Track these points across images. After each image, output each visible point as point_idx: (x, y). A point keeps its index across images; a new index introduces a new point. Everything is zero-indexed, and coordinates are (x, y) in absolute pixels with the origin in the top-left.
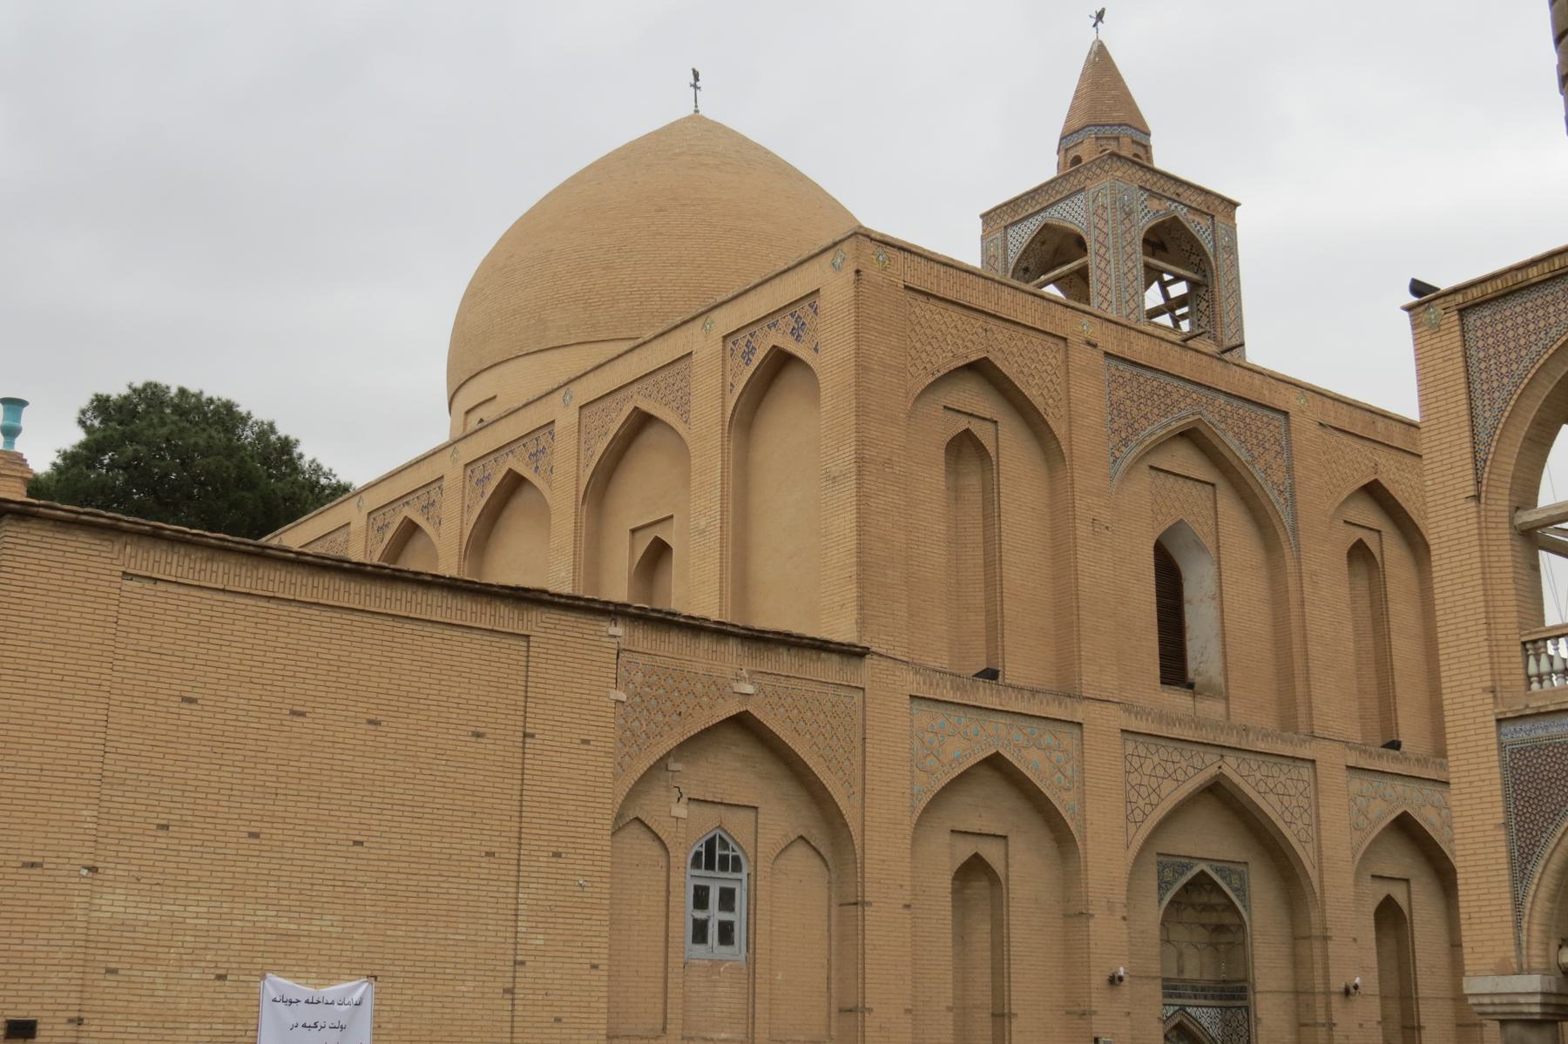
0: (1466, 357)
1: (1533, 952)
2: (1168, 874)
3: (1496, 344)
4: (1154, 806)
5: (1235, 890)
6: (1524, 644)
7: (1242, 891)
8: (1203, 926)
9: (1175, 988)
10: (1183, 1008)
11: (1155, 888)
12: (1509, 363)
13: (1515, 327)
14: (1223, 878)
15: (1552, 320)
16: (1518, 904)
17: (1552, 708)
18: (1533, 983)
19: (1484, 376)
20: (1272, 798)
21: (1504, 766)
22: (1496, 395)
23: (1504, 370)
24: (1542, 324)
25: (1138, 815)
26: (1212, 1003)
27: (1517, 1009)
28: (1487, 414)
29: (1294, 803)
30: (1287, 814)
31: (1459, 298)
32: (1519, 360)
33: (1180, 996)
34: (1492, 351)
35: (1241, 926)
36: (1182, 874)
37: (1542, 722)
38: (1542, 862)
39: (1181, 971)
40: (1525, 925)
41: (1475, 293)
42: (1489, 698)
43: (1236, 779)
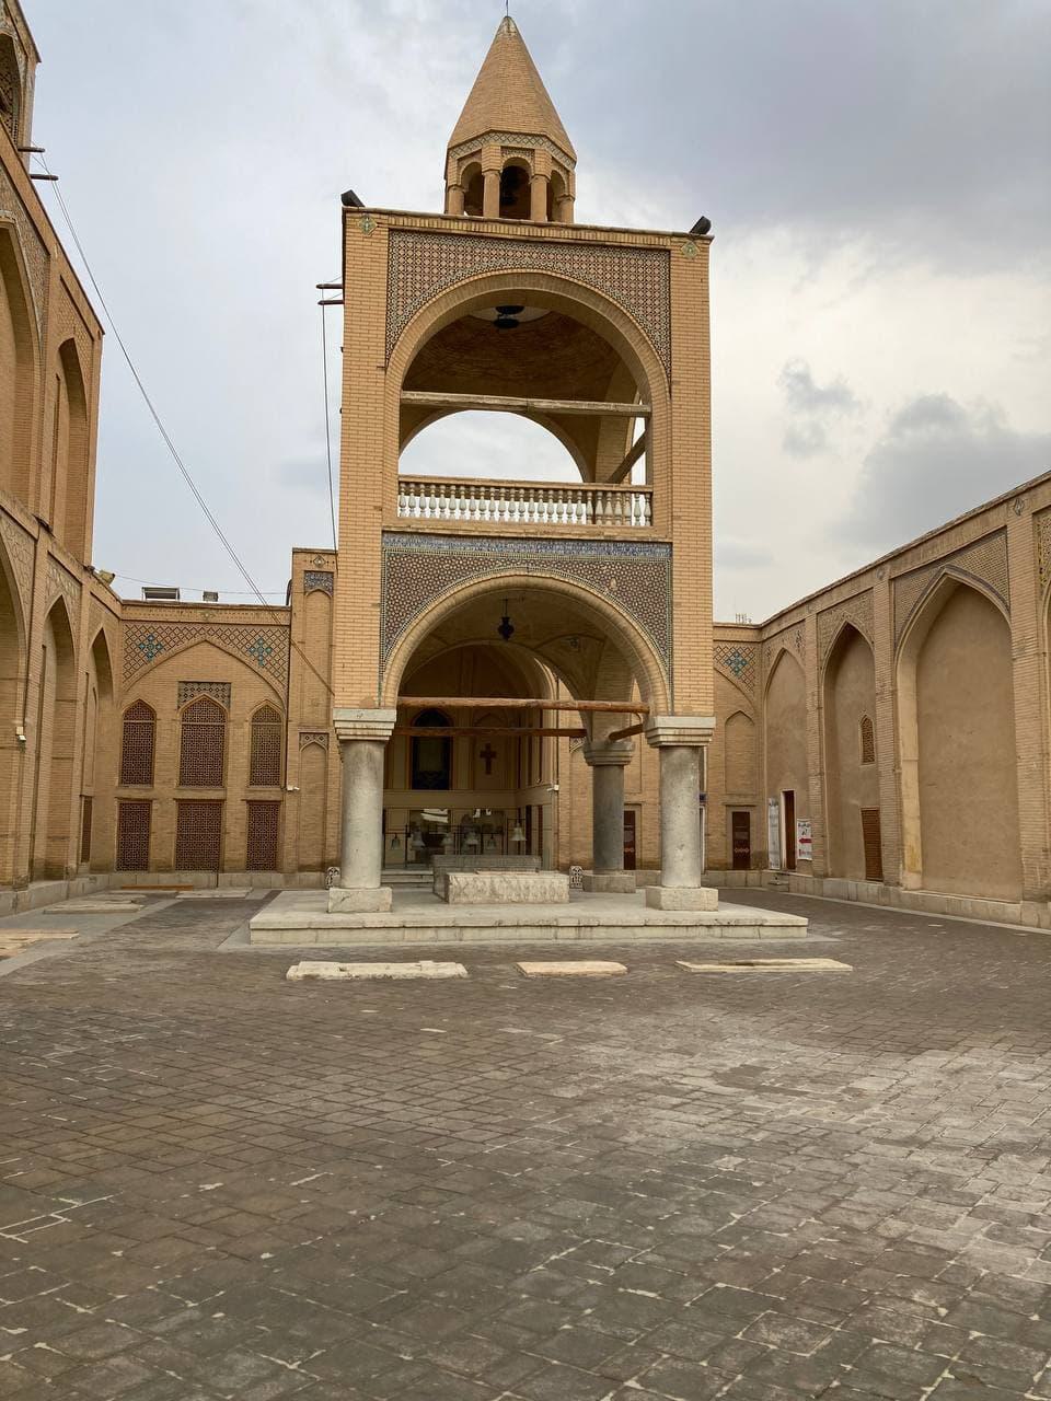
0: (389, 266)
1: (389, 695)
3: (414, 265)
6: (400, 482)
12: (422, 282)
13: (431, 258)
15: (460, 265)
16: (382, 661)
17: (427, 531)
18: (392, 715)
19: (401, 284)
21: (383, 564)
22: (409, 301)
23: (418, 286)
24: (452, 264)
27: (371, 732)
28: (400, 312)
31: (393, 220)
32: (431, 283)
34: (410, 269)
37: (417, 539)
38: (405, 634)
40: (385, 676)
41: (407, 222)
42: (378, 514)
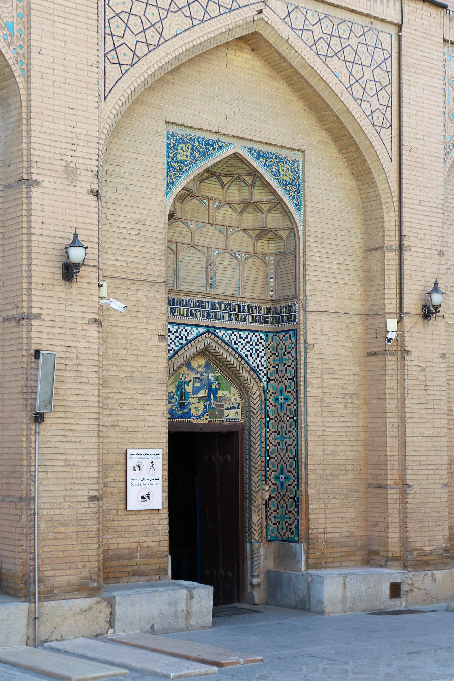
2: (184, 153)
4: (152, 48)
5: (284, 183)
7: (295, 186)
8: (245, 230)
9: (201, 304)
10: (211, 330)
11: (163, 167)
14: (266, 166)
20: (334, 63)
25: (125, 55)
26: (255, 326)
29: (368, 75)
30: (356, 87)
33: (208, 316)
35: (292, 230)
36: (206, 154)
39: (210, 283)
43: (285, 31)
